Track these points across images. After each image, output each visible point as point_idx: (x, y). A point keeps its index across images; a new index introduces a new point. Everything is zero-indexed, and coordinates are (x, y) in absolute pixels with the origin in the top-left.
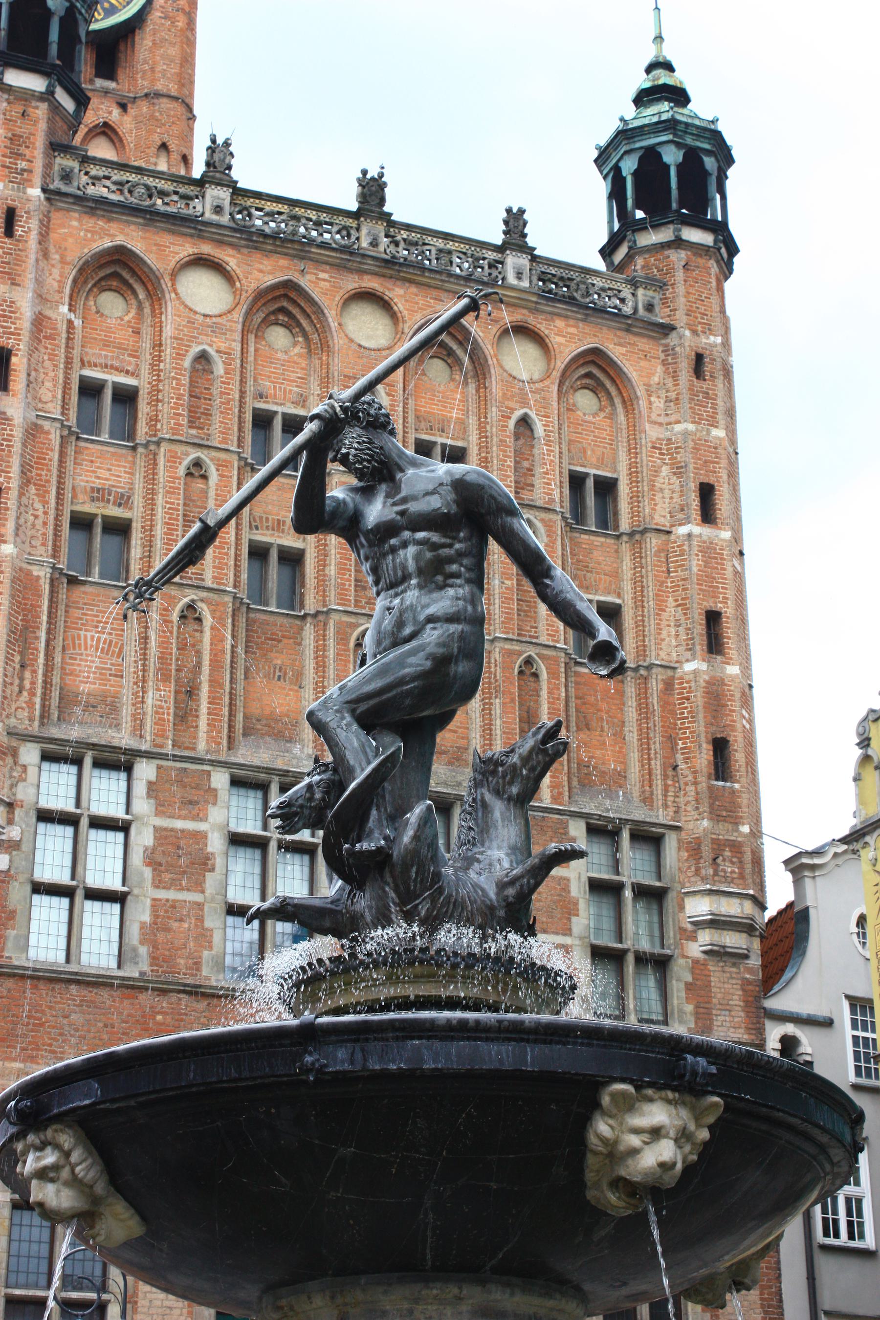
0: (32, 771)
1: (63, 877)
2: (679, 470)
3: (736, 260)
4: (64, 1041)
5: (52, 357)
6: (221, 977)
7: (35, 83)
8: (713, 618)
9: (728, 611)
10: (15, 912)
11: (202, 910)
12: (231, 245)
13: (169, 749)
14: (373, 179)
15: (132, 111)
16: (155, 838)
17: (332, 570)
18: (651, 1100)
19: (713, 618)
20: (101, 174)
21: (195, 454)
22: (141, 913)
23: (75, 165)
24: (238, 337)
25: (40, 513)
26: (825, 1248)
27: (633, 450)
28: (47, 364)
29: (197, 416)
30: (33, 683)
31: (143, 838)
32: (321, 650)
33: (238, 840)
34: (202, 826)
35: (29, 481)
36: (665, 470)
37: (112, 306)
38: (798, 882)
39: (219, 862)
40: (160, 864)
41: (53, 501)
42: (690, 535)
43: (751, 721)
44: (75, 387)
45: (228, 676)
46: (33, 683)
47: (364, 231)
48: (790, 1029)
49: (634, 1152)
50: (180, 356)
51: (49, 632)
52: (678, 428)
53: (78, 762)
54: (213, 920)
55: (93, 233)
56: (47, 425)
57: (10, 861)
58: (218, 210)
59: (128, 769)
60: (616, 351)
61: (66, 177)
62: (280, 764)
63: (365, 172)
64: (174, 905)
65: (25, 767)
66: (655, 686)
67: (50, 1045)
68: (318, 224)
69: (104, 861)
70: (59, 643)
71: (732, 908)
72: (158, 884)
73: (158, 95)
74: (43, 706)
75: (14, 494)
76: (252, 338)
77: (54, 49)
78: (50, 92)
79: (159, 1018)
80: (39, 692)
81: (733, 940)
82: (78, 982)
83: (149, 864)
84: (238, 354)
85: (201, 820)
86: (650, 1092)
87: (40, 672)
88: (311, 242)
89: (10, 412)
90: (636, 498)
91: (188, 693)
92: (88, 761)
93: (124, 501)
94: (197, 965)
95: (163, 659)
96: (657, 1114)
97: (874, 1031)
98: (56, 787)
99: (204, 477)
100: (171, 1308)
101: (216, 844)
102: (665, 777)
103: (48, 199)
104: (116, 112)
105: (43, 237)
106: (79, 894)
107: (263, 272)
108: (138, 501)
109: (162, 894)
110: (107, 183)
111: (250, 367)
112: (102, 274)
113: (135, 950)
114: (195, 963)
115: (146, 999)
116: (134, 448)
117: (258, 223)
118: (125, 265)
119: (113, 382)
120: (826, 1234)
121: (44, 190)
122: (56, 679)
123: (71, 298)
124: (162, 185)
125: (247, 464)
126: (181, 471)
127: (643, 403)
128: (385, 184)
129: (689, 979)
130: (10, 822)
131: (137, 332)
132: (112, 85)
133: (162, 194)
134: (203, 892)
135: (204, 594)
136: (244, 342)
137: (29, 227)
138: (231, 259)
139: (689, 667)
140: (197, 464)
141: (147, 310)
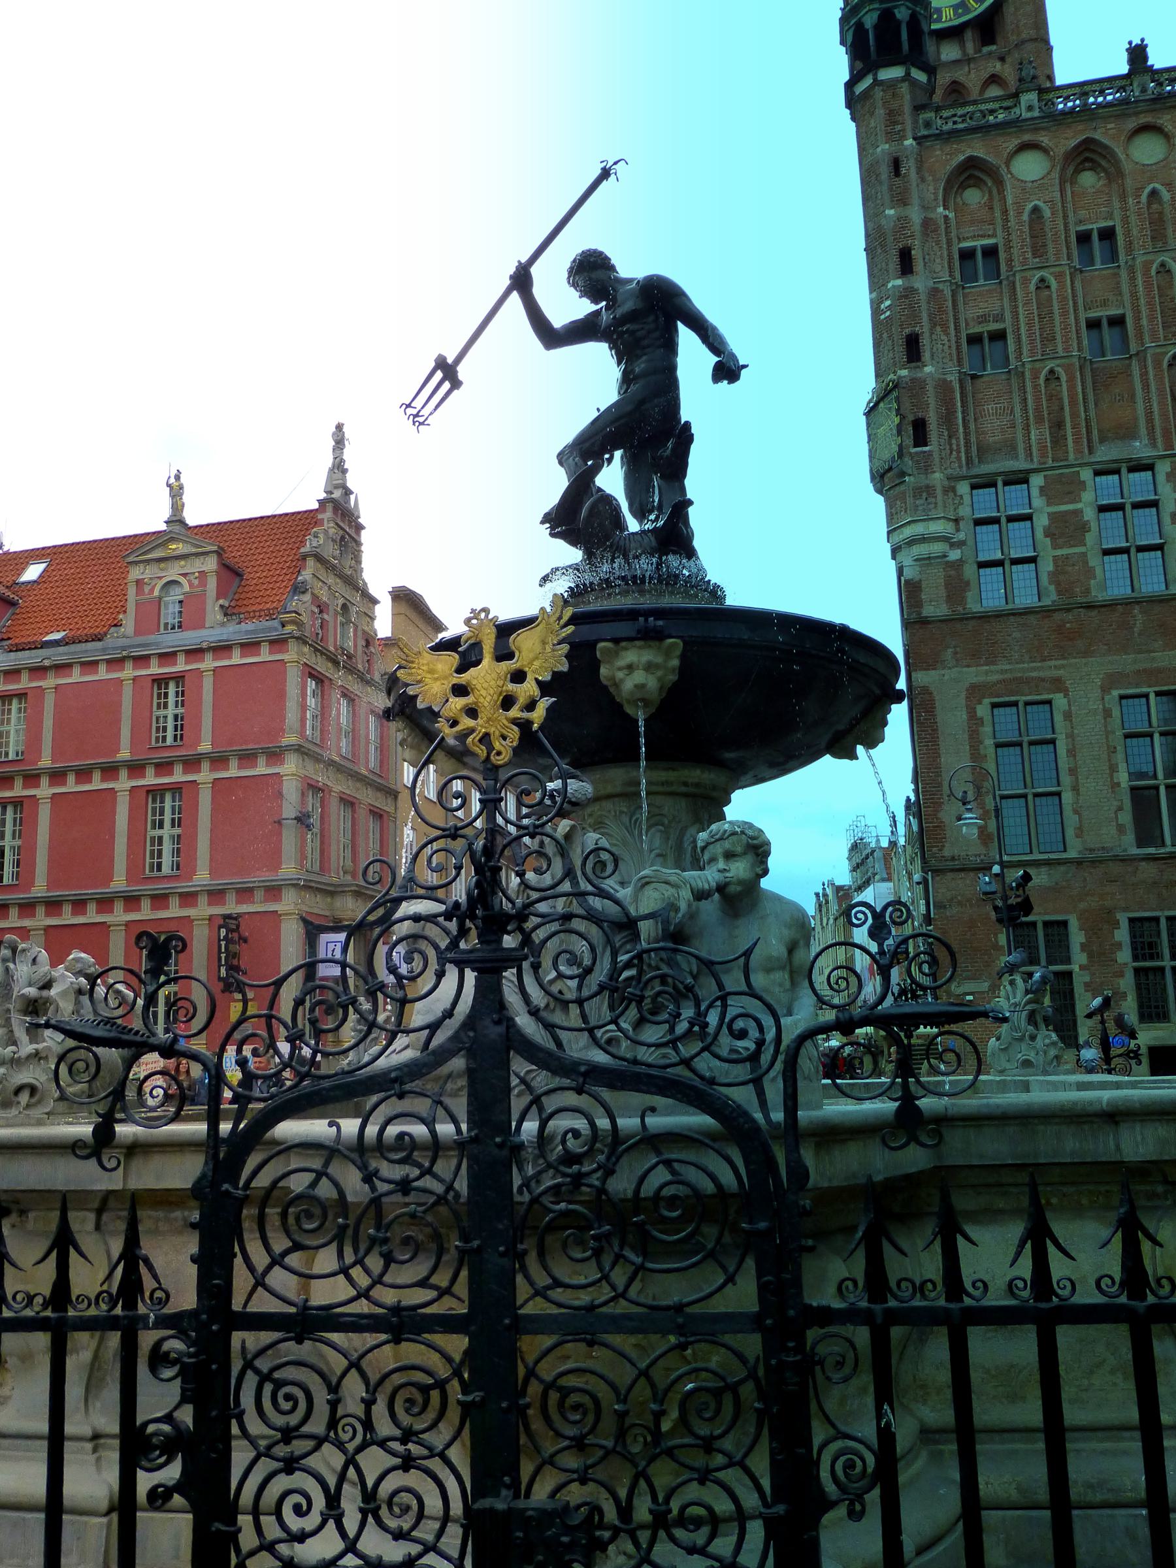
0: (967, 499)
5: (938, 243)
7: (896, 72)
12: (1043, 129)
13: (1050, 463)
14: (1137, 45)
15: (1009, 60)
17: (1144, 322)
18: (626, 649)
20: (950, 114)
21: (1039, 274)
22: (1046, 566)
23: (932, 114)
24: (1057, 188)
25: (946, 342)
28: (936, 248)
29: (1038, 250)
30: (958, 445)
31: (1041, 521)
32: (1144, 374)
33: (1103, 509)
34: (1079, 506)
35: (935, 325)
37: (973, 196)
39: (1094, 525)
41: (953, 332)
44: (956, 256)
45: (1082, 409)
46: (958, 445)
47: (1135, 86)
49: (622, 681)
50: (1020, 213)
51: (963, 412)
53: (994, 485)
54: (1094, 561)
55: (951, 155)
56: (941, 286)
58: (1030, 108)
59: (1026, 481)
61: (928, 124)
62: (1125, 455)
63: (1130, 43)
64: (1067, 557)
65: (961, 496)
68: (1102, 92)
69: (1019, 542)
70: (971, 417)
72: (1055, 546)
73: (1023, 42)
74: (967, 458)
75: (926, 335)
76: (1068, 185)
77: (905, 46)
78: (908, 74)
80: (963, 450)
82: (1014, 614)
83: (1046, 536)
84: (1059, 199)
86: (624, 644)
87: (962, 437)
88: (1100, 105)
89: (917, 285)
91: (1058, 425)
92: (1000, 484)
93: (999, 318)
94: (1088, 591)
95: (1038, 409)
96: (631, 656)
98: (984, 502)
99: (1048, 287)
101: (1089, 514)
103: (918, 144)
104: (998, 65)
105: (919, 170)
107: (1070, 139)
108: (1008, 315)
109: (1059, 552)
110: (956, 119)
111: (1070, 206)
112: (961, 179)
113: (1046, 588)
115: (1057, 616)
116: (1001, 283)
117: (1061, 106)
118: (974, 167)
119: (982, 246)
121: (914, 139)
122: (973, 439)
123: (944, 201)
124: (991, 106)
125: (1076, 270)
126: (1032, 287)
128: (1146, 46)
130: (958, 530)
131: (991, 208)
132: (994, 48)
133: (992, 112)
135: (1058, 362)
136: (1062, 191)
137: (909, 168)
138: (1044, 139)
140: (1042, 280)
141: (995, 191)
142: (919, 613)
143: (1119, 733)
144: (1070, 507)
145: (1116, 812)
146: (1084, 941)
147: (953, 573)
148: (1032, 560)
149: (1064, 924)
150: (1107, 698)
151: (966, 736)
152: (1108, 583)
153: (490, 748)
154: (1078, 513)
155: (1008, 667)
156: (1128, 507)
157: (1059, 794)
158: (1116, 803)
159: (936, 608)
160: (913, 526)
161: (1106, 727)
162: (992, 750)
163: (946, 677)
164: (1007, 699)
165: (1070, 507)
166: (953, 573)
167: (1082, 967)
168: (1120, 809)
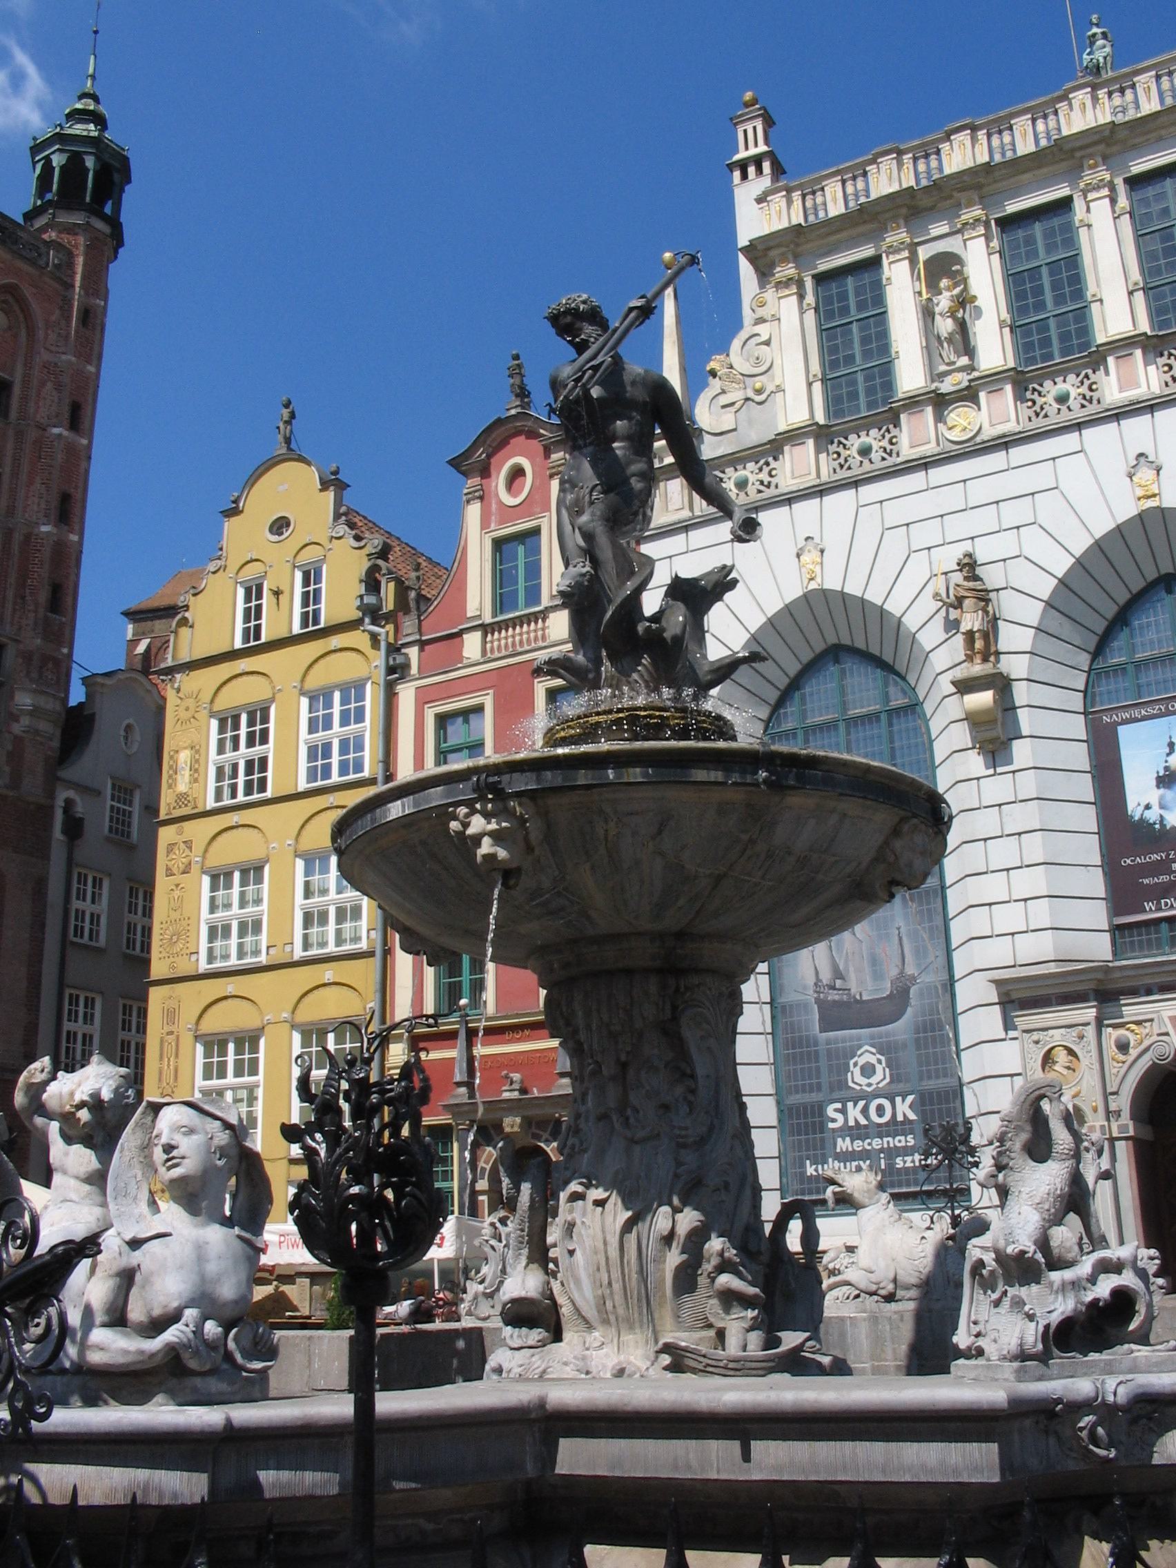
2: (59, 387)
3: (121, 250)
8: (65, 499)
9: (79, 496)
19: (65, 499)
26: (73, 943)
27: (28, 365)
36: (49, 385)
38: (89, 695)
42: (60, 435)
43: (78, 575)
48: (71, 794)
52: (64, 357)
60: (27, 291)
66: (17, 537)
71: (50, 705)
81: (44, 726)
90: (24, 398)
97: (130, 806)
102: (15, 603)
120: (75, 936)
127: (41, 334)
129: (10, 748)
139: (44, 529)
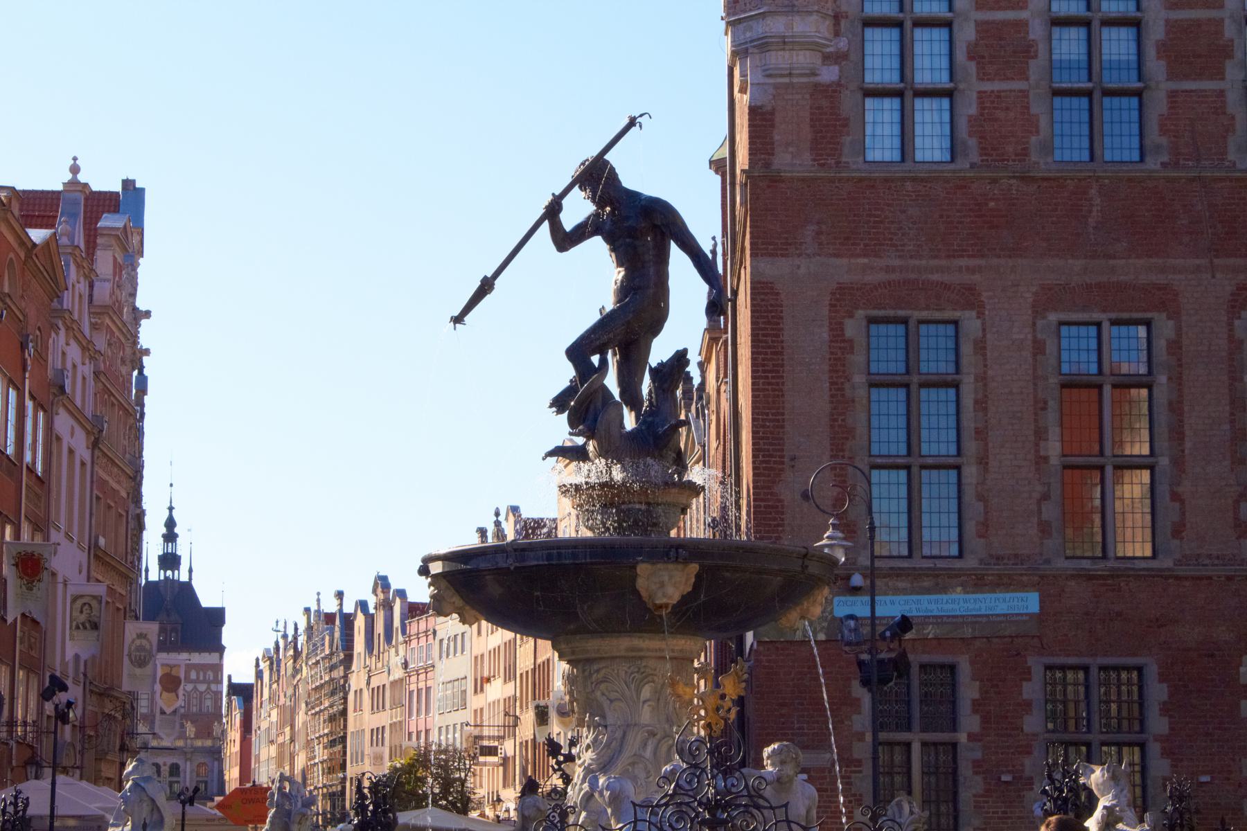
1: (891, 78)
4: (903, 235)
6: (1050, 160)
10: (847, 119)
11: (1027, 97)
16: (977, 31)
34: (1024, 15)
39: (1042, 48)
40: (983, 57)
57: (840, 71)
64: (998, 95)
67: (891, 239)
72: (983, 76)
79: (992, 204)
83: (971, 58)
85: (1022, 8)
94: (1025, 153)
100: (1019, 467)
106: (909, 94)
109: (988, 87)
114: (1024, 149)
134: (1027, 79)
142: (767, 165)
143: (1054, 380)
144: (1010, 15)
145: (1039, 502)
146: (976, 696)
147: (825, 103)
148: (949, 94)
149: (952, 668)
150: (1040, 323)
151: (827, 368)
152: (1057, 142)
153: (711, 729)
154: (1020, 26)
155: (897, 262)
156: (1096, 24)
157: (958, 468)
158: (1039, 488)
159: (793, 161)
160: (769, 21)
161: (1035, 369)
162: (862, 392)
163: (803, 271)
164: (891, 313)
165: (1010, 15)
166: (825, 103)
167: (972, 737)
168: (1045, 497)
